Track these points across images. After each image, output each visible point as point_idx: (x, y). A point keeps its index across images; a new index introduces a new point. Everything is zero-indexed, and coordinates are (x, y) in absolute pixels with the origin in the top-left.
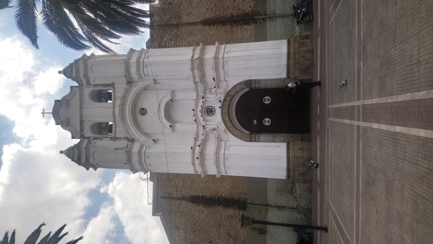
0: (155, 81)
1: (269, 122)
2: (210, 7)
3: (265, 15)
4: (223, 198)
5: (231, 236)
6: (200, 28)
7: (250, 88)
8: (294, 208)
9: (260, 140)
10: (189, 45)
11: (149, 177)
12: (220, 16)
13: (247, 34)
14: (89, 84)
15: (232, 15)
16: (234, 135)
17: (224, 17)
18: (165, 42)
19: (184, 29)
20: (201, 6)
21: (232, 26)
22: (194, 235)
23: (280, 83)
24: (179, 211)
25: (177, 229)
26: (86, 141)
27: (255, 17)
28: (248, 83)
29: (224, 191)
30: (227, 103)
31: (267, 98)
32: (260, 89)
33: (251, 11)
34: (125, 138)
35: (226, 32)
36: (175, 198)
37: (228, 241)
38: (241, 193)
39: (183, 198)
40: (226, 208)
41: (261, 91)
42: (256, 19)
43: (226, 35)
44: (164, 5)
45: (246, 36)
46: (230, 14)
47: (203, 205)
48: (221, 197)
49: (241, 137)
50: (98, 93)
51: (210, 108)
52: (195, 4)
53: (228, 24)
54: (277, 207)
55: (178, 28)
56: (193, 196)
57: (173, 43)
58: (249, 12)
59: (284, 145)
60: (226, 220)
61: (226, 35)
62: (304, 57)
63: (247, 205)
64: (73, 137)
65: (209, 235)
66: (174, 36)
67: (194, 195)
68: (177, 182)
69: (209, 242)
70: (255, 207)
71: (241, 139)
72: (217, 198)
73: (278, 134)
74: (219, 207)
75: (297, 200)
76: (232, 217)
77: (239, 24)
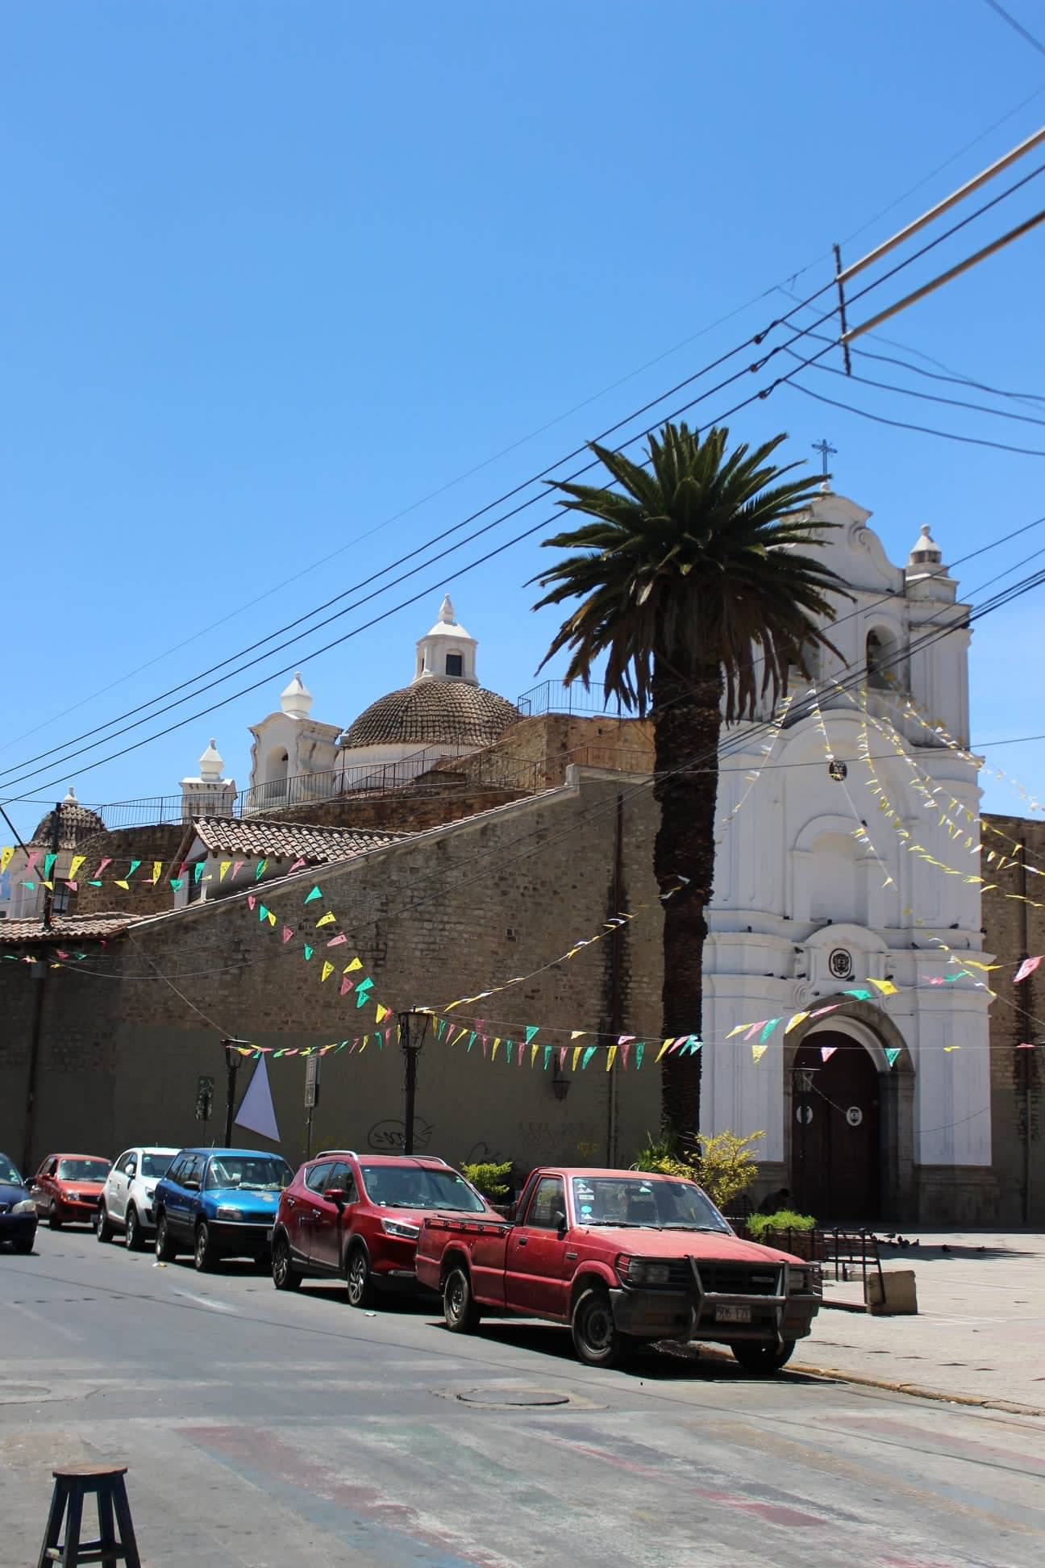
11: (573, 713)
14: (910, 629)
28: (906, 1069)
30: (863, 1014)
39: (619, 864)
41: (875, 1103)
42: (1025, 1094)
50: (875, 637)
53: (1019, 1025)
59: (779, 1156)
65: (529, 934)
67: (628, 898)
69: (509, 932)
72: (626, 965)
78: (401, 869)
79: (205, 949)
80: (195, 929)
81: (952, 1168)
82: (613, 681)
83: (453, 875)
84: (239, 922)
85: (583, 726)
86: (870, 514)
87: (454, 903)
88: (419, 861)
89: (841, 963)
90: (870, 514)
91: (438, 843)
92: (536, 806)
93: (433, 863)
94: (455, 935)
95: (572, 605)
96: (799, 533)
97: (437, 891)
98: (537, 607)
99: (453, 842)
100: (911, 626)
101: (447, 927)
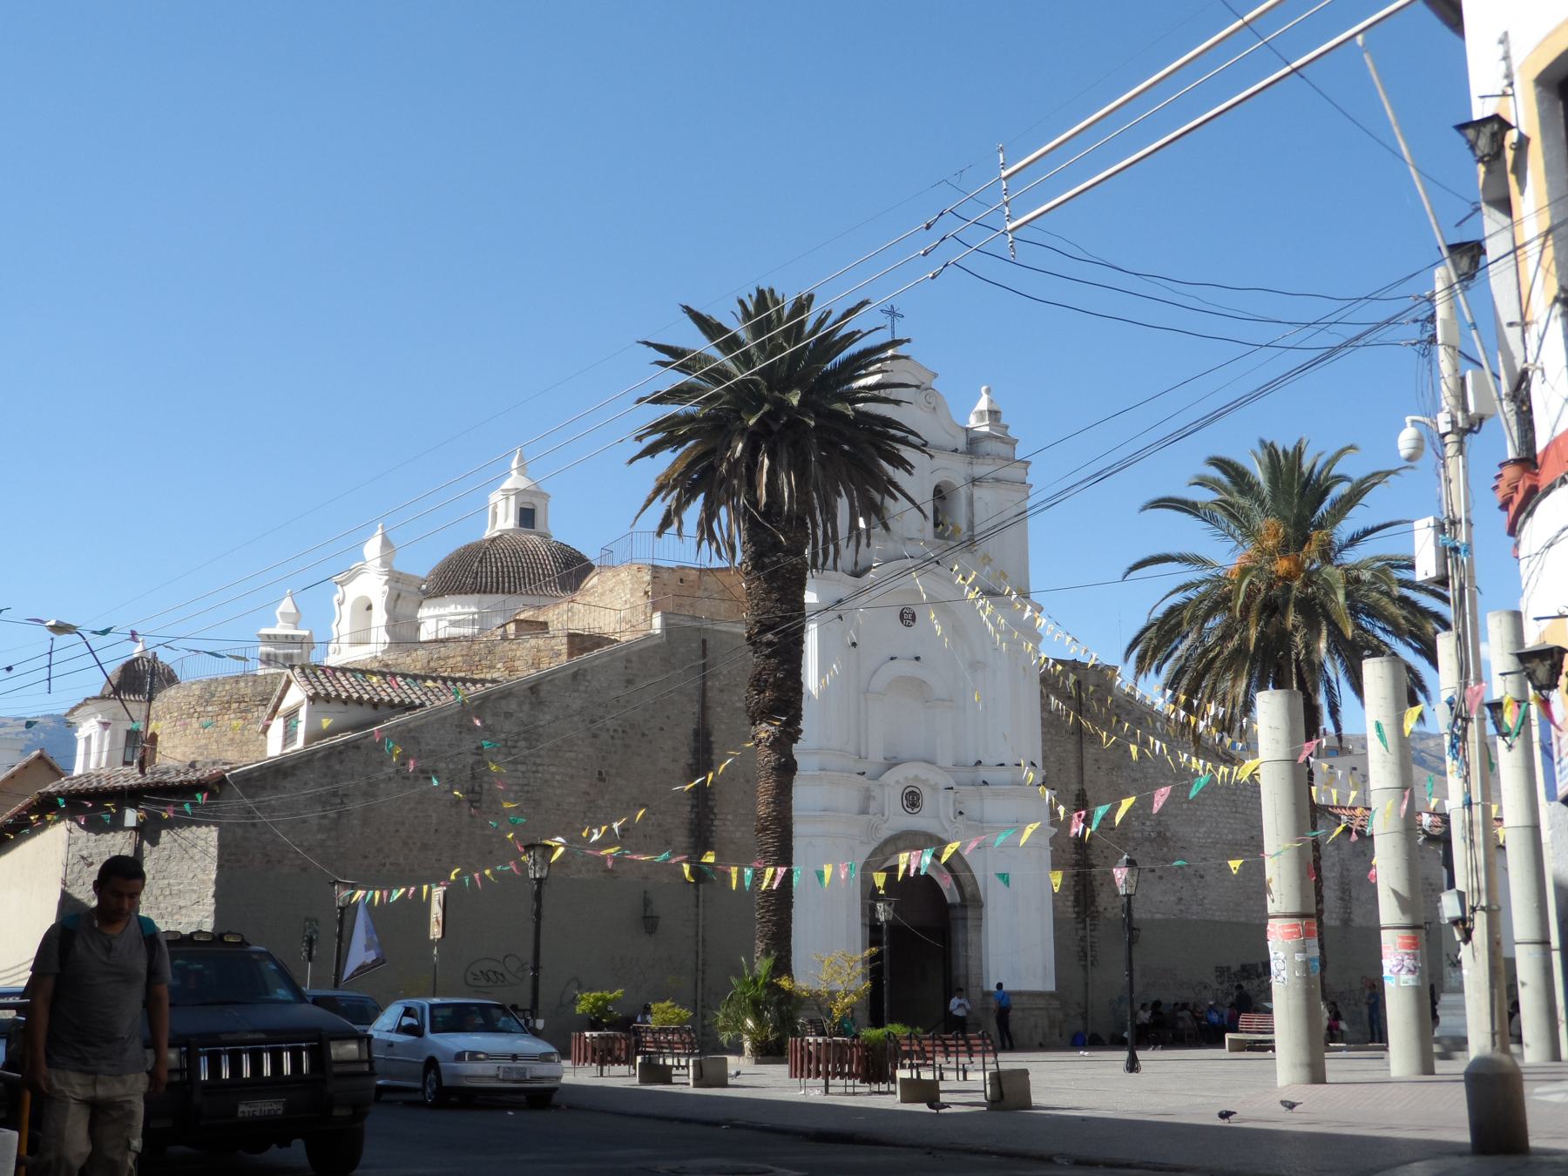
0: (975, 666)
7: (963, 906)
10: (1045, 758)
15: (1093, 866)
19: (1071, 746)
21: (1073, 866)
34: (856, 563)
39: (704, 708)
42: (1084, 921)
62: (1036, 1026)
78: (495, 715)
80: (293, 775)
82: (706, 528)
84: (337, 767)
85: (666, 575)
86: (936, 375)
88: (513, 705)
89: (912, 800)
90: (936, 375)
91: (531, 688)
93: (526, 707)
95: (667, 458)
96: (883, 393)
97: (530, 734)
98: (631, 461)
99: (545, 688)
100: (974, 481)
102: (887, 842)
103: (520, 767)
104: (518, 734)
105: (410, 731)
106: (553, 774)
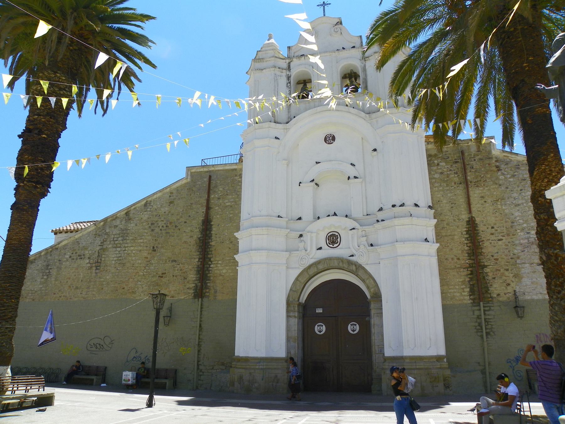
1: (320, 332)
2: (496, 230)
3: (485, 319)
4: (210, 265)
5: (162, 277)
6: (463, 217)
8: (198, 365)
9: (290, 319)
12: (482, 249)
13: (455, 292)
15: (486, 266)
16: (297, 279)
17: (481, 253)
18: (438, 165)
19: (460, 191)
20: (496, 217)
22: (162, 226)
23: (376, 347)
24: (192, 204)
25: (171, 203)
26: (285, 66)
27: (481, 303)
28: (378, 296)
29: (218, 268)
30: (346, 266)
31: (357, 328)
32: (369, 315)
33: (491, 297)
34: (289, 118)
35: (459, 259)
36: (209, 196)
37: (155, 274)
38: (216, 292)
39: (208, 208)
40: (196, 269)
42: (479, 305)
43: (453, 259)
44: (495, 159)
45: (452, 291)
46: (486, 264)
47: (199, 236)
48: (210, 263)
49: (294, 289)
50: (355, 73)
51: (339, 240)
52: (500, 207)
53: (471, 262)
54: (199, 342)
55: (460, 183)
56: (211, 221)
57: (437, 176)
58: (490, 294)
60: (181, 270)
61: (453, 259)
63: (200, 299)
64: (289, 48)
65: (162, 247)
66: (448, 177)
67: (212, 223)
68: (230, 197)
69: (153, 247)
70: (198, 310)
71: (291, 290)
72: (209, 256)
73: (301, 346)
74: (197, 260)
75: (210, 371)
76: (185, 278)
77: (471, 279)
78: (110, 227)
79: (37, 270)
81: (402, 358)
83: (131, 226)
87: (131, 238)
88: (118, 222)
90: (340, 18)
91: (126, 213)
92: (169, 189)
93: (123, 222)
94: (130, 252)
97: (124, 233)
101: (127, 249)
102: (310, 266)
103: (118, 249)
104: (119, 234)
105: (76, 239)
106: (132, 250)
